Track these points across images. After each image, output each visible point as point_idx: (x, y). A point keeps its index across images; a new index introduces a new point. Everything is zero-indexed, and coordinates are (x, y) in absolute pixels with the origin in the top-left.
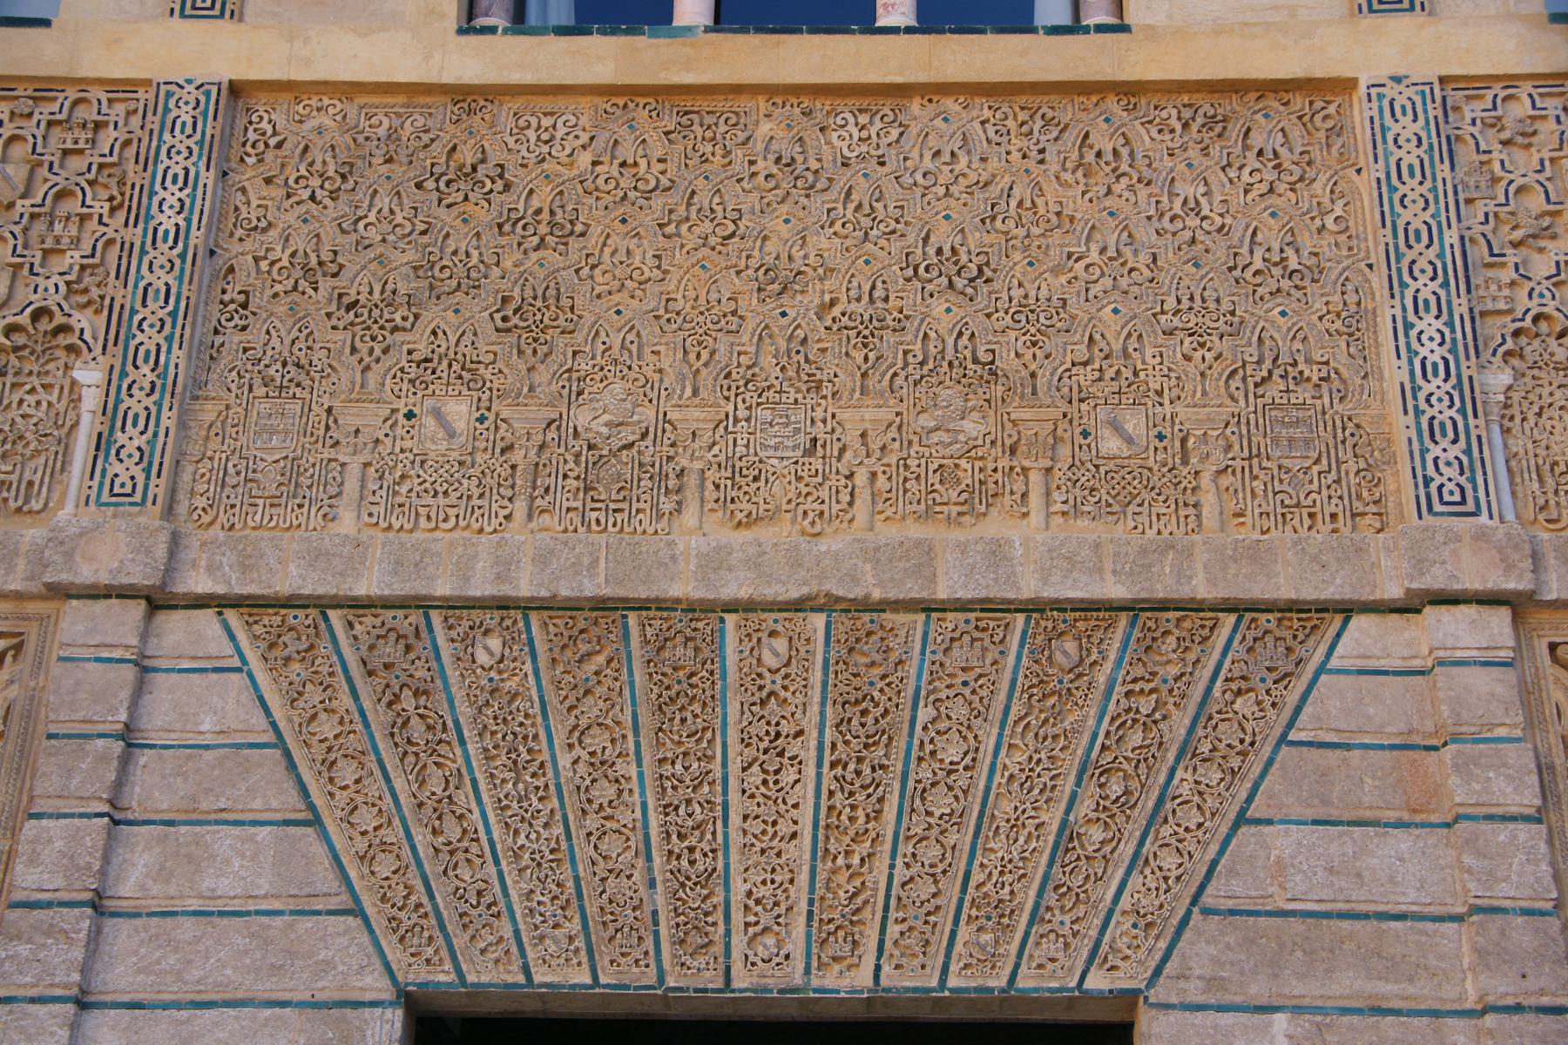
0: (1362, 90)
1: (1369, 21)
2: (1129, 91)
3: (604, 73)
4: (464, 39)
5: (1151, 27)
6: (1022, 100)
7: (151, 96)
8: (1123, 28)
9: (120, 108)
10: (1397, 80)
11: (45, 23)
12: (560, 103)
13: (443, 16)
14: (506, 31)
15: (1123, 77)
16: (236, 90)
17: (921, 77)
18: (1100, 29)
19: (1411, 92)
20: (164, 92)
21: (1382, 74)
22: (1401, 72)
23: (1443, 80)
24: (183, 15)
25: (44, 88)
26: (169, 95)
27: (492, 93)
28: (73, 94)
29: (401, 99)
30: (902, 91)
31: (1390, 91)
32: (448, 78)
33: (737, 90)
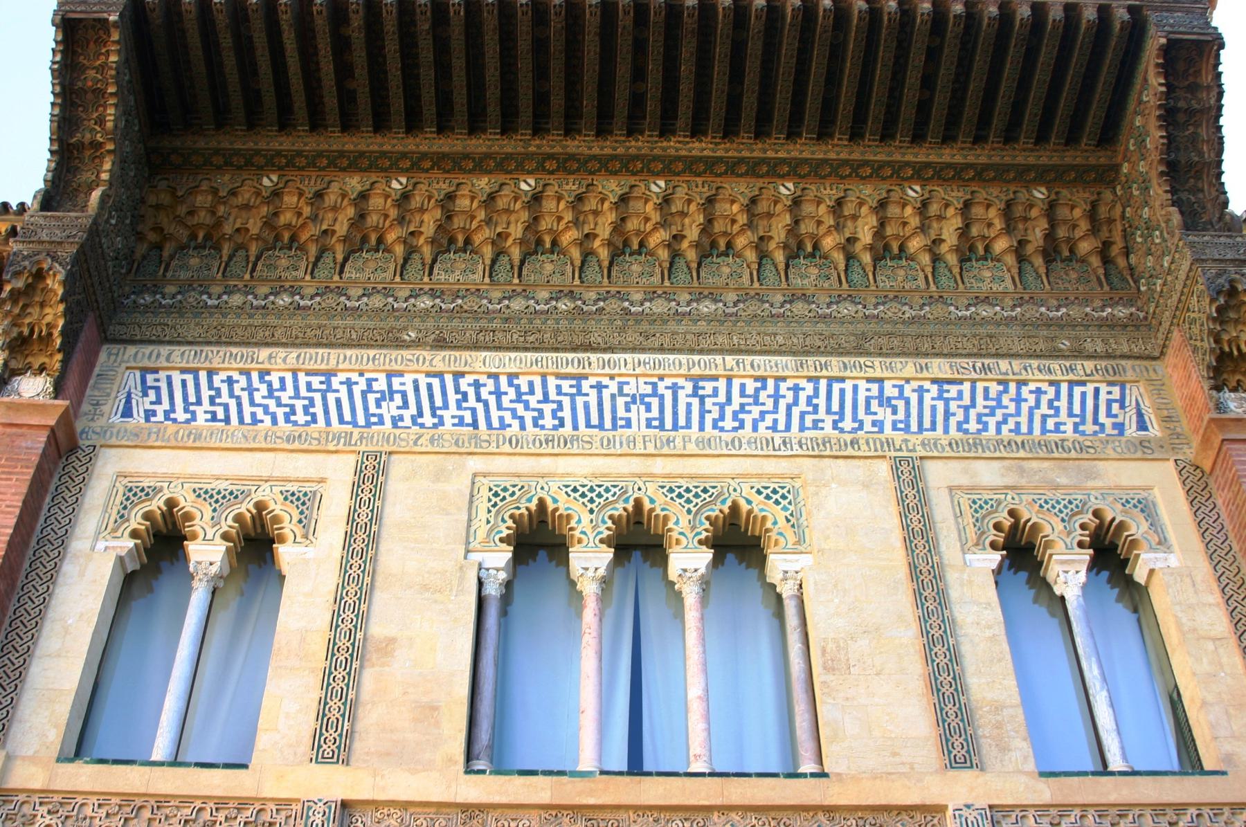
0: (950, 813)
1: (952, 773)
2: (829, 810)
3: (545, 797)
4: (469, 777)
5: (839, 774)
6: (773, 814)
7: (299, 807)
8: (823, 775)
9: (283, 814)
10: (968, 806)
11: (245, 766)
12: (521, 812)
13: (456, 762)
14: (491, 773)
15: (826, 803)
16: (345, 805)
17: (718, 802)
18: (813, 775)
19: (975, 813)
20: (307, 805)
21: (960, 803)
22: (970, 802)
23: (991, 807)
24: (317, 762)
25: (243, 804)
26: (309, 808)
27: (482, 808)
28: (258, 806)
29: (433, 810)
30: (709, 809)
31: (965, 813)
32: (460, 800)
33: (618, 807)
